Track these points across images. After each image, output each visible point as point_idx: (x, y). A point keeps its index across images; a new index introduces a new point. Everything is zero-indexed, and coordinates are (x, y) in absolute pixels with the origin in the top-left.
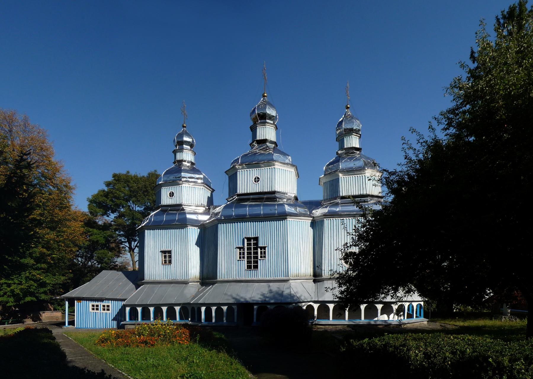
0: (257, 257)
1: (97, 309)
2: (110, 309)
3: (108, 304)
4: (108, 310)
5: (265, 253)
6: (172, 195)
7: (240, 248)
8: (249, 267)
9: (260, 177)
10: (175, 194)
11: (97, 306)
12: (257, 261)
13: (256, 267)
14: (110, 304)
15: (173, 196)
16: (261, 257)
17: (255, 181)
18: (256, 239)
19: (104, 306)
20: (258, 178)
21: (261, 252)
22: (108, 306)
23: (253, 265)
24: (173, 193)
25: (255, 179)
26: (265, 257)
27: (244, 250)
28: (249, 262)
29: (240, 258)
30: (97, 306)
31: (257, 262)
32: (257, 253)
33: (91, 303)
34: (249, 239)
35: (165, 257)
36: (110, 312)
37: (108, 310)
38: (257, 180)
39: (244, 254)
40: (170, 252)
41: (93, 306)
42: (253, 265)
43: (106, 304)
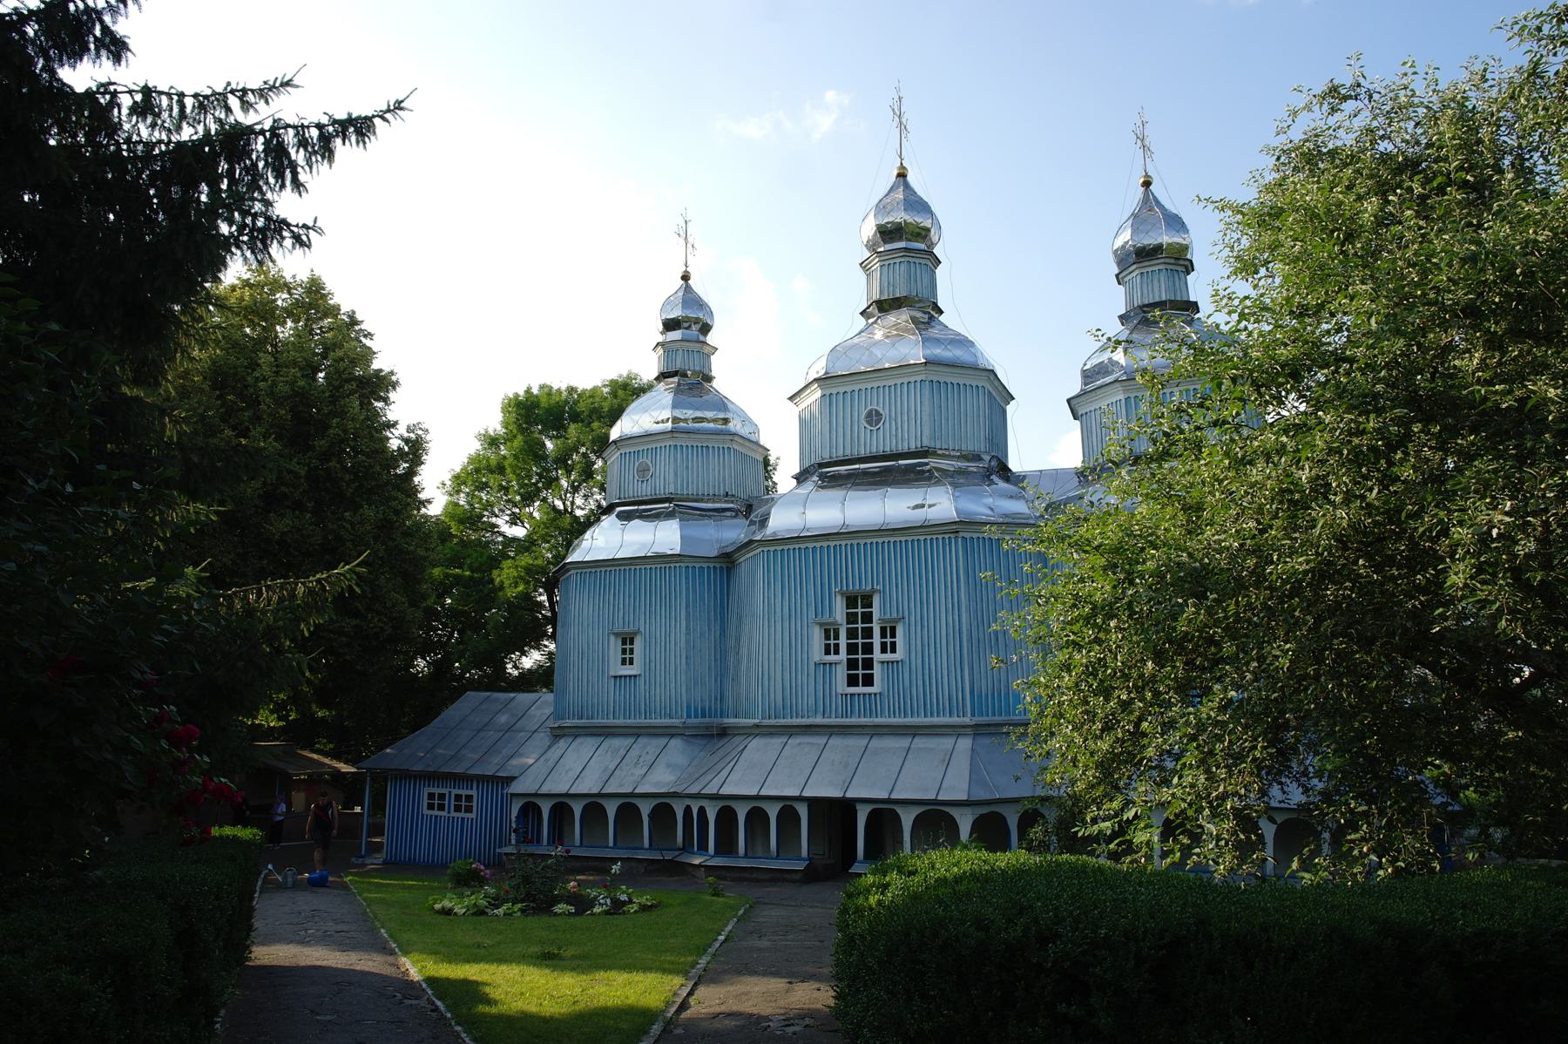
1: (441, 807)
3: (469, 792)
4: (469, 810)
6: (643, 470)
11: (442, 796)
14: (473, 792)
16: (884, 650)
17: (870, 423)
19: (458, 797)
22: (469, 798)
25: (869, 415)
33: (427, 791)
36: (473, 815)
38: (874, 417)
41: (431, 796)
43: (464, 792)
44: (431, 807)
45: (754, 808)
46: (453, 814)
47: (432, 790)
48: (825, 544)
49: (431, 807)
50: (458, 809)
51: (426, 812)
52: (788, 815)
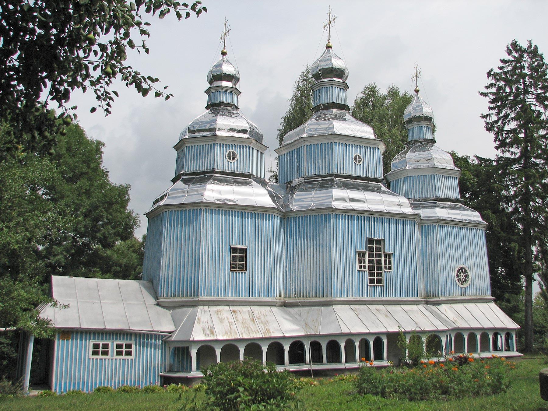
0: (380, 268)
1: (105, 353)
2: (133, 353)
3: (129, 342)
5: (390, 262)
6: (232, 157)
7: (360, 254)
8: (371, 281)
9: (361, 156)
10: (237, 157)
12: (381, 273)
13: (380, 281)
15: (234, 158)
16: (386, 268)
17: (356, 161)
18: (378, 242)
20: (359, 157)
21: (385, 261)
23: (376, 279)
24: (234, 154)
25: (356, 157)
26: (390, 268)
27: (364, 256)
28: (371, 274)
29: (360, 267)
30: (105, 346)
31: (380, 275)
32: (379, 262)
33: (92, 342)
34: (370, 241)
35: (234, 258)
36: (133, 357)
37: (129, 353)
38: (358, 159)
39: (364, 263)
40: (243, 251)
41: (96, 346)
42: (376, 279)
44: (95, 353)
45: (362, 340)
46: (115, 357)
47: (96, 342)
48: (362, 215)
49: (95, 353)
50: (119, 353)
51: (92, 357)
52: (378, 343)
